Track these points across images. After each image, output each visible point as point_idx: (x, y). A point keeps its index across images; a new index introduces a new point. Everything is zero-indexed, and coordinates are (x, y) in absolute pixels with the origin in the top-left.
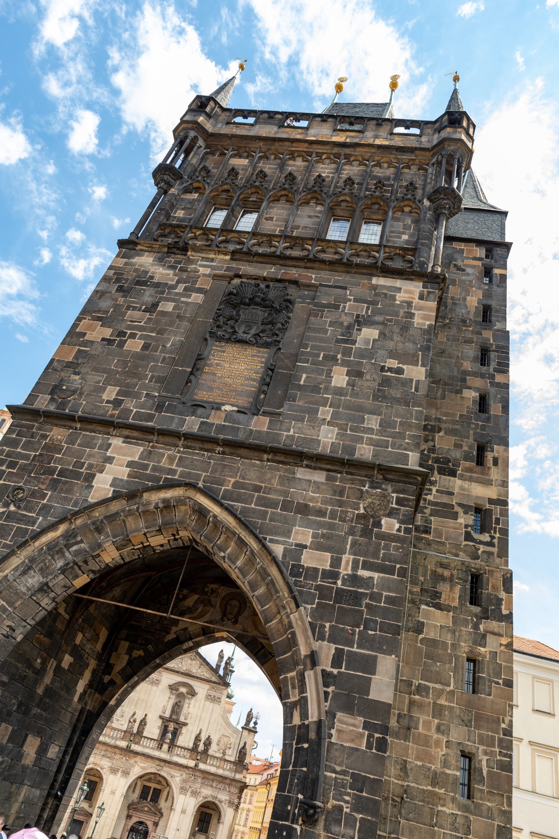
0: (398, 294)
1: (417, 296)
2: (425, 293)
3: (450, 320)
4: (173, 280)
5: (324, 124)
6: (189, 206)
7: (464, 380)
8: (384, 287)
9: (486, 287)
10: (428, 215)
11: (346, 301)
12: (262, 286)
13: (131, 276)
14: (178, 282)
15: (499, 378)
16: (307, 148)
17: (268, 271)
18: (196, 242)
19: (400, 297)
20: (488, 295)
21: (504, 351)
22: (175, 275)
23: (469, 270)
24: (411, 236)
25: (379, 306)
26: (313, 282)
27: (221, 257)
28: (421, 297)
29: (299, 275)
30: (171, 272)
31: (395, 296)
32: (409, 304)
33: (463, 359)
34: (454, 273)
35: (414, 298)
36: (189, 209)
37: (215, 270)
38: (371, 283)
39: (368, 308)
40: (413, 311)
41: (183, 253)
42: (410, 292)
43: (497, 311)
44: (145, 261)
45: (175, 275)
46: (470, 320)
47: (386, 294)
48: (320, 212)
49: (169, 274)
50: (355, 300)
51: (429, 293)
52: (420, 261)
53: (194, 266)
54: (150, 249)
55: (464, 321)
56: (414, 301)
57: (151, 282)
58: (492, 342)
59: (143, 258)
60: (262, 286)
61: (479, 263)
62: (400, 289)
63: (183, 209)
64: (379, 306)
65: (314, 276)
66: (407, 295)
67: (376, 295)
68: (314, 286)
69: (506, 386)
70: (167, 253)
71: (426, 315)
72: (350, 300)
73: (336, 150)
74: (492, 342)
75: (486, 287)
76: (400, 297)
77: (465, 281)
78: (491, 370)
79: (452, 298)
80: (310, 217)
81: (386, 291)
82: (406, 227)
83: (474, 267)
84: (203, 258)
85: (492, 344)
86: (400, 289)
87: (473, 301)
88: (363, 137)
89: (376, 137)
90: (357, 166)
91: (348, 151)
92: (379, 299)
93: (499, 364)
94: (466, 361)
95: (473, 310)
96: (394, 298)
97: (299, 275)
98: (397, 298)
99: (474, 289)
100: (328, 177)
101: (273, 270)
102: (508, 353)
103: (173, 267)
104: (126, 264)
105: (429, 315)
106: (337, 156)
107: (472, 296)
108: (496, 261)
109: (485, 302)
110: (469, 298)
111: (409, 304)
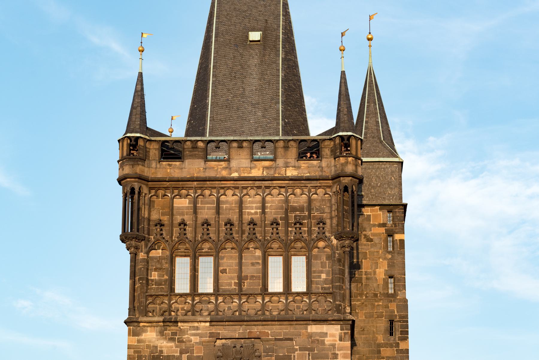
0: (326, 339)
1: (338, 338)
2: (343, 334)
3: (366, 297)
4: (177, 352)
5: (240, 151)
6: (159, 266)
7: (379, 352)
8: (316, 333)
9: (390, 256)
10: (337, 255)
11: (295, 350)
12: (238, 347)
13: (146, 352)
14: (181, 353)
15: (402, 346)
16: (234, 184)
17: (238, 331)
18: (177, 306)
19: (328, 341)
20: (391, 265)
21: (405, 319)
22: (176, 347)
23: (376, 240)
24: (327, 275)
25: (316, 352)
26: (270, 337)
27: (203, 324)
28: (341, 340)
29: (260, 332)
30: (172, 344)
31: (324, 340)
32: (334, 346)
33: (377, 334)
34: (365, 245)
35: (336, 341)
36: (160, 269)
37: (202, 337)
38: (307, 332)
39: (309, 354)
40: (337, 352)
41: (175, 324)
42: (333, 335)
43: (399, 280)
44: (151, 336)
45: (176, 347)
46: (380, 293)
47: (318, 340)
48: (259, 257)
49: (172, 347)
50: (301, 349)
51: (345, 334)
52: (336, 304)
53: (186, 336)
54: (150, 324)
55: (376, 295)
56: (337, 343)
57: (162, 356)
58: (396, 313)
59: (148, 333)
60: (238, 347)
61: (382, 230)
62: (327, 333)
63: (156, 270)
64: (316, 352)
65: (269, 332)
66: (331, 339)
67: (313, 342)
68: (271, 340)
69: (407, 351)
70: (164, 326)
71: (345, 354)
72: (296, 350)
73: (257, 183)
74: (396, 313)
75: (390, 256)
76: (327, 341)
77: (373, 252)
78: (397, 339)
79: (366, 273)
80: (253, 264)
81: (318, 338)
82: (323, 265)
83: (380, 234)
84: (190, 327)
85: (396, 315)
86: (327, 333)
87: (381, 273)
88: (276, 168)
89: (287, 166)
90: (277, 197)
91: (267, 183)
92: (315, 345)
93: (402, 332)
94: (379, 334)
95: (382, 282)
96: (323, 342)
97: (260, 332)
98: (326, 343)
99: (381, 260)
100: (256, 213)
101: (241, 331)
102: (407, 322)
103: (172, 339)
104: (139, 341)
105: (347, 353)
106: (259, 187)
107: (380, 268)
108: (396, 226)
109: (390, 273)
110: (377, 270)
111: (334, 346)
